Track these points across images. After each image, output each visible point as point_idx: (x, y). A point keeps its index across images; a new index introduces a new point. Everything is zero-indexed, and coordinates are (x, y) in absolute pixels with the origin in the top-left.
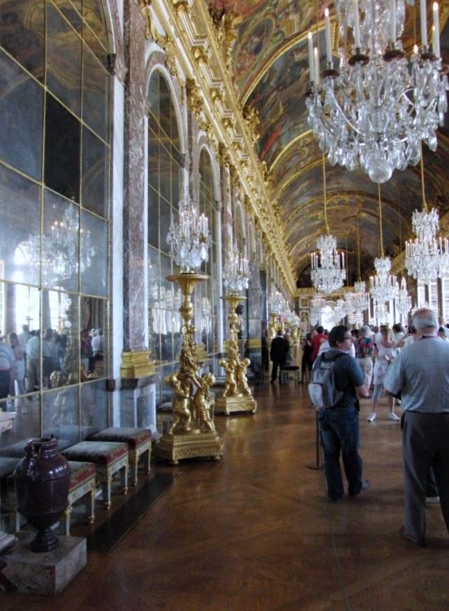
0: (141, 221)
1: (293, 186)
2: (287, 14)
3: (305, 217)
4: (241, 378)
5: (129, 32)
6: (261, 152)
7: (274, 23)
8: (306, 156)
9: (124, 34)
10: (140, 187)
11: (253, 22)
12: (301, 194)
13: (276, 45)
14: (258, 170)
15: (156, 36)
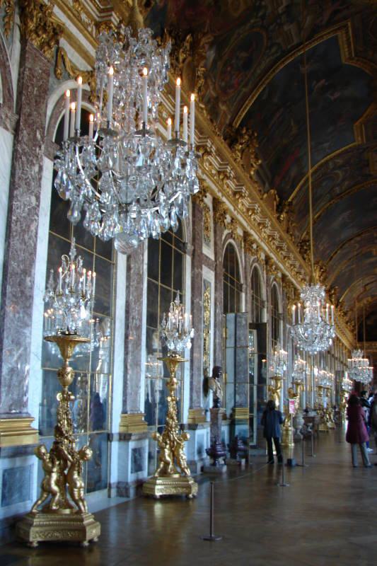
0: (30, 276)
3: (355, 253)
4: (179, 455)
5: (23, 78)
9: (19, 81)
10: (30, 238)
14: (261, 202)
15: (74, 73)
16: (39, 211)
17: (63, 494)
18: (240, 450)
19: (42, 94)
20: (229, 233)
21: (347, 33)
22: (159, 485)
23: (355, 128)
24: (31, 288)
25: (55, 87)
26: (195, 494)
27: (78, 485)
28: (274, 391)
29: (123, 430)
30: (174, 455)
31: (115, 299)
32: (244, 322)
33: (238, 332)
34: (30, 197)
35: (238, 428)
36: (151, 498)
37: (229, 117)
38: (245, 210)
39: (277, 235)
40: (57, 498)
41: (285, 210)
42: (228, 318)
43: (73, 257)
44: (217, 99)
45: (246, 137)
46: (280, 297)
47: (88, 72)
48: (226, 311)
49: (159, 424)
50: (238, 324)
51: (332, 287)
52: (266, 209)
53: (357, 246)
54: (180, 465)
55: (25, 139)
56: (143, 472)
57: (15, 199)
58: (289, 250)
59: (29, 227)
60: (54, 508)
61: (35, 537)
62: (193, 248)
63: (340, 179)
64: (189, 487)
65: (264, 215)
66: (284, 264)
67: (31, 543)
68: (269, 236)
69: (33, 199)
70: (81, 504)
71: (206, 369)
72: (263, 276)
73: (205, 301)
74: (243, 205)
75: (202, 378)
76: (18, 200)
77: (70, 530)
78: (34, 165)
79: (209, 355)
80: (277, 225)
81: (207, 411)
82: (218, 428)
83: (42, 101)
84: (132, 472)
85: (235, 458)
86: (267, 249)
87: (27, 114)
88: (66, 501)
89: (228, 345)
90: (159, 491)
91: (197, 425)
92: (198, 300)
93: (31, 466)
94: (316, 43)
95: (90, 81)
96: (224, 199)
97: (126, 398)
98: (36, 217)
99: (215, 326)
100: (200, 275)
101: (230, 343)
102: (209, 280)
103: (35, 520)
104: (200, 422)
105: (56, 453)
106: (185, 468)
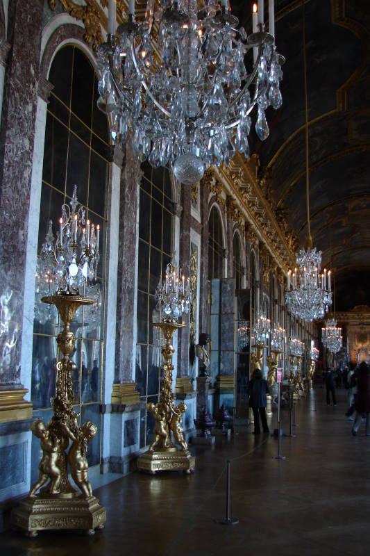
0: (22, 229)
4: (176, 427)
8: (317, 148)
10: (23, 187)
14: (245, 166)
16: (32, 156)
17: (64, 477)
18: (226, 420)
19: (36, 24)
20: (213, 197)
22: (155, 459)
24: (24, 243)
25: (49, 18)
26: (192, 469)
27: (82, 465)
28: (257, 360)
29: (115, 400)
30: (170, 428)
31: (108, 259)
32: (229, 288)
33: (222, 299)
34: (23, 141)
35: (223, 397)
36: (148, 475)
40: (58, 481)
41: (265, 176)
42: (213, 284)
43: (74, 208)
46: (257, 264)
47: (83, 7)
48: (210, 278)
49: (157, 397)
50: (223, 291)
54: (176, 438)
55: (18, 73)
56: (136, 445)
57: (7, 141)
58: (267, 217)
59: (22, 173)
60: (55, 492)
61: (35, 525)
62: (182, 210)
64: (187, 462)
65: (246, 180)
66: (261, 230)
67: (30, 532)
68: (249, 202)
69: (27, 142)
70: (85, 487)
71: (193, 336)
72: (243, 240)
73: (191, 266)
74: (227, 168)
75: (189, 345)
76: (11, 143)
77: (74, 517)
78: (27, 103)
79: (195, 321)
80: (258, 190)
81: (193, 380)
82: (205, 397)
83: (36, 31)
84: (125, 447)
85: (221, 428)
86: (246, 214)
87: (20, 44)
88: (68, 483)
89: (212, 312)
90: (156, 464)
91: (185, 395)
92: (186, 263)
93: (25, 444)
95: (84, 17)
97: (119, 367)
98: (30, 164)
99: (201, 292)
100: (188, 237)
101: (215, 310)
102: (195, 243)
103: (34, 507)
104: (188, 391)
105: (56, 429)
106: (182, 441)
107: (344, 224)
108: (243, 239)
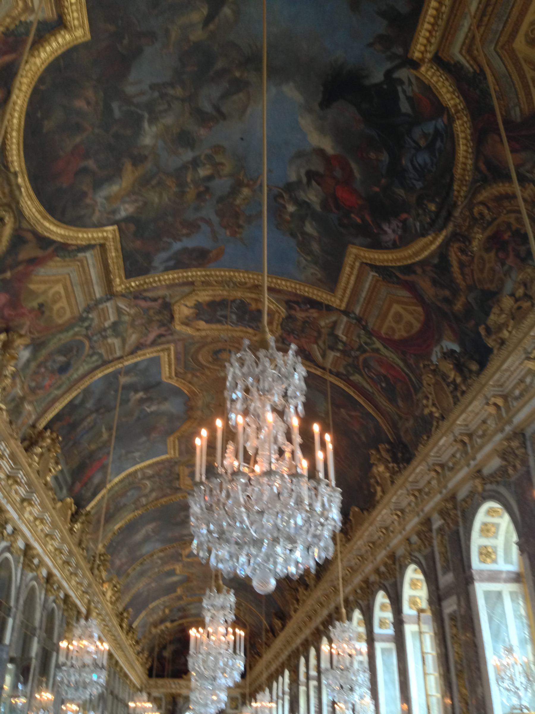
1: (131, 528)
2: (105, 337)
6: (73, 483)
7: (87, 344)
11: (55, 340)
12: (147, 539)
13: (91, 366)
14: (53, 512)
21: (169, 355)
23: (168, 441)
37: (34, 417)
38: (32, 519)
39: (65, 548)
41: (80, 520)
44: (23, 399)
45: (49, 441)
46: (57, 623)
51: (125, 609)
52: (57, 518)
53: (159, 562)
58: (78, 566)
63: (147, 490)
68: (56, 549)
72: (40, 595)
86: (50, 564)
94: (139, 359)
96: (9, 508)
107: (178, 572)
108: (40, 593)
